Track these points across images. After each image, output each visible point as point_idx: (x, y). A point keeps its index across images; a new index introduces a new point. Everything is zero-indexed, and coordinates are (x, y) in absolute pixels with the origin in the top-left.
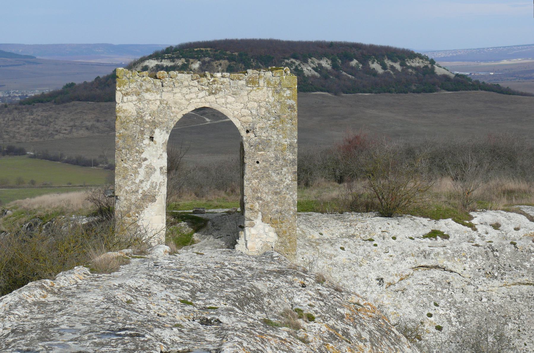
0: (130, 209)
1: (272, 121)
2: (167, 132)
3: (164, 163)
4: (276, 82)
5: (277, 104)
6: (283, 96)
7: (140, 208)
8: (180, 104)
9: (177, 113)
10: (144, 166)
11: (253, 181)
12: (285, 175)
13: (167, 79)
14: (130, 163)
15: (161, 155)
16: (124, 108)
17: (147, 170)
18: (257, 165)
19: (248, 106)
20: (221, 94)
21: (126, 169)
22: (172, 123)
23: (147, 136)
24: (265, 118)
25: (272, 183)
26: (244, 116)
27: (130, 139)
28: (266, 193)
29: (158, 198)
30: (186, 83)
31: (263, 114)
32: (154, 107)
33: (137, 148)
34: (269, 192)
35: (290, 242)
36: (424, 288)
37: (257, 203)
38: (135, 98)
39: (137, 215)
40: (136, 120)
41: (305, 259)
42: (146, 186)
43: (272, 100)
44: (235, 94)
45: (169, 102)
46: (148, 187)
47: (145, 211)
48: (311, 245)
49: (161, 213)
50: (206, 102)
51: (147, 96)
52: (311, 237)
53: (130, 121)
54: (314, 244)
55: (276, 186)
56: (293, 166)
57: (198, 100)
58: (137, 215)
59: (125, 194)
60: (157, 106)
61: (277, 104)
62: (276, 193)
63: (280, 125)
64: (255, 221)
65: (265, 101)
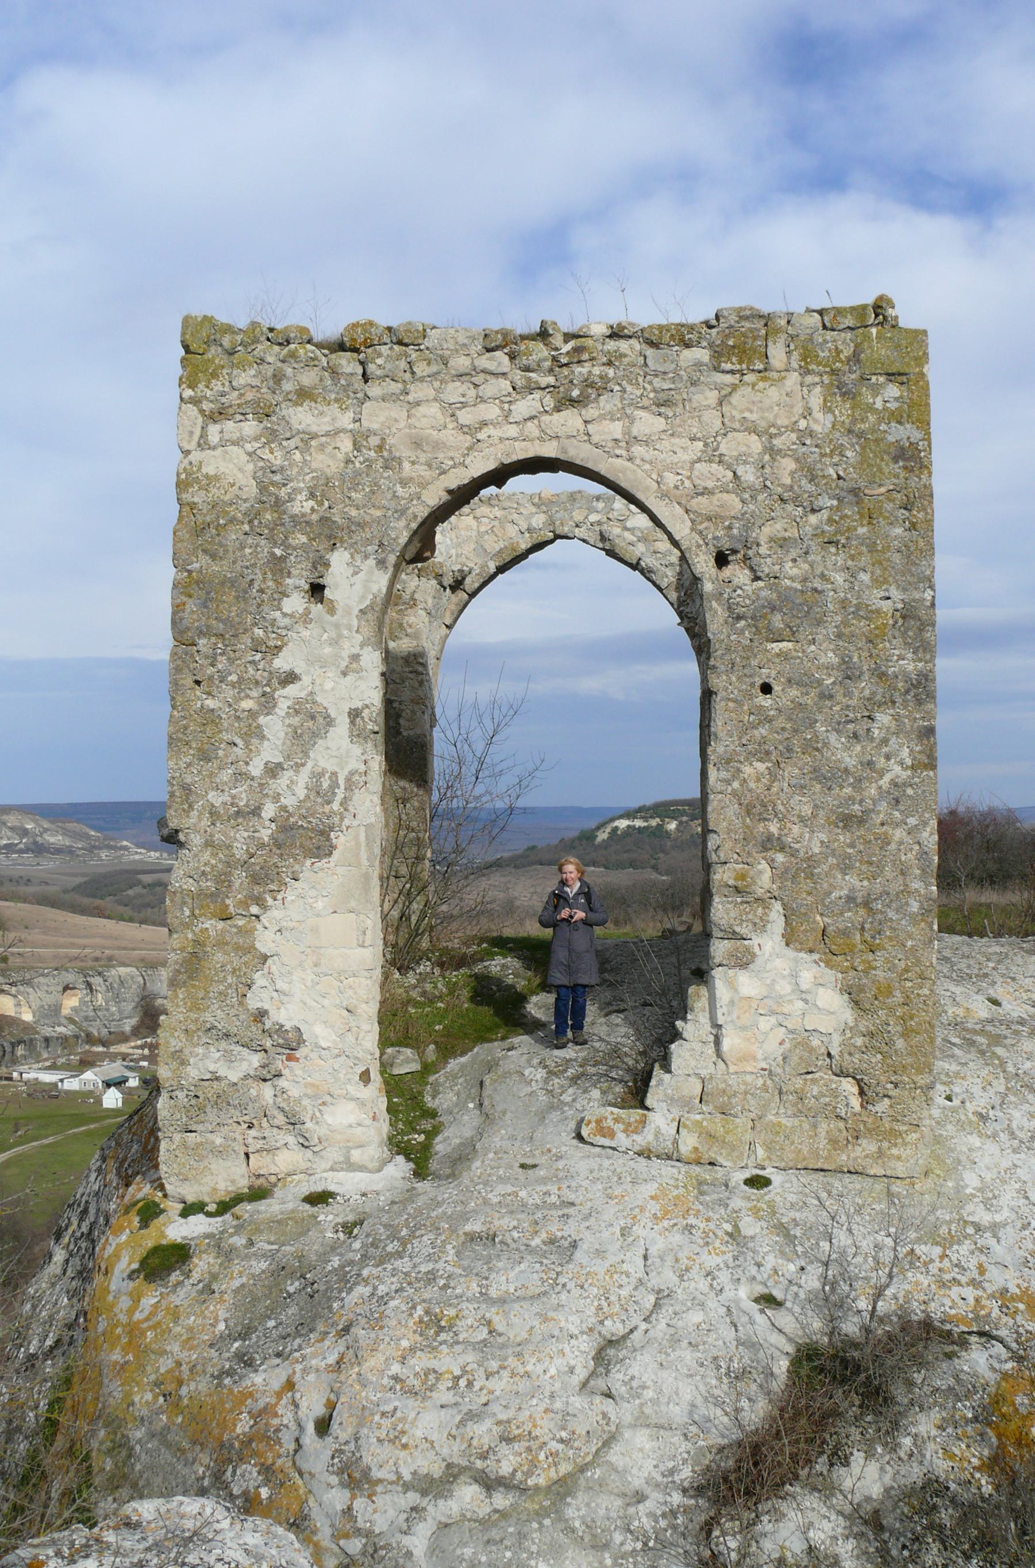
0: (223, 880)
1: (825, 515)
2: (381, 563)
3: (369, 691)
4: (838, 352)
5: (844, 441)
6: (871, 408)
7: (265, 880)
8: (437, 446)
9: (423, 485)
11: (747, 770)
12: (885, 741)
13: (384, 349)
14: (229, 693)
15: (355, 658)
16: (209, 469)
17: (296, 721)
18: (765, 701)
19: (723, 449)
20: (607, 403)
22: (402, 523)
23: (298, 580)
24: (797, 501)
25: (828, 777)
26: (706, 492)
27: (230, 596)
28: (802, 819)
29: (341, 840)
30: (461, 363)
31: (788, 481)
32: (326, 462)
33: (259, 632)
34: (814, 816)
35: (905, 1035)
37: (764, 865)
38: (250, 427)
39: (254, 910)
40: (252, 516)
41: (956, 1102)
42: (293, 790)
43: (821, 422)
44: (667, 403)
45: (390, 441)
46: (301, 793)
47: (290, 895)
48: (972, 1043)
49: (353, 904)
50: (546, 436)
51: (301, 417)
52: (961, 1012)
53: (232, 520)
54: (981, 1040)
55: (848, 791)
57: (512, 431)
58: (254, 910)
59: (205, 822)
60: (341, 456)
61: (844, 441)
62: (847, 821)
63: (862, 530)
64: (756, 941)
65: (793, 427)
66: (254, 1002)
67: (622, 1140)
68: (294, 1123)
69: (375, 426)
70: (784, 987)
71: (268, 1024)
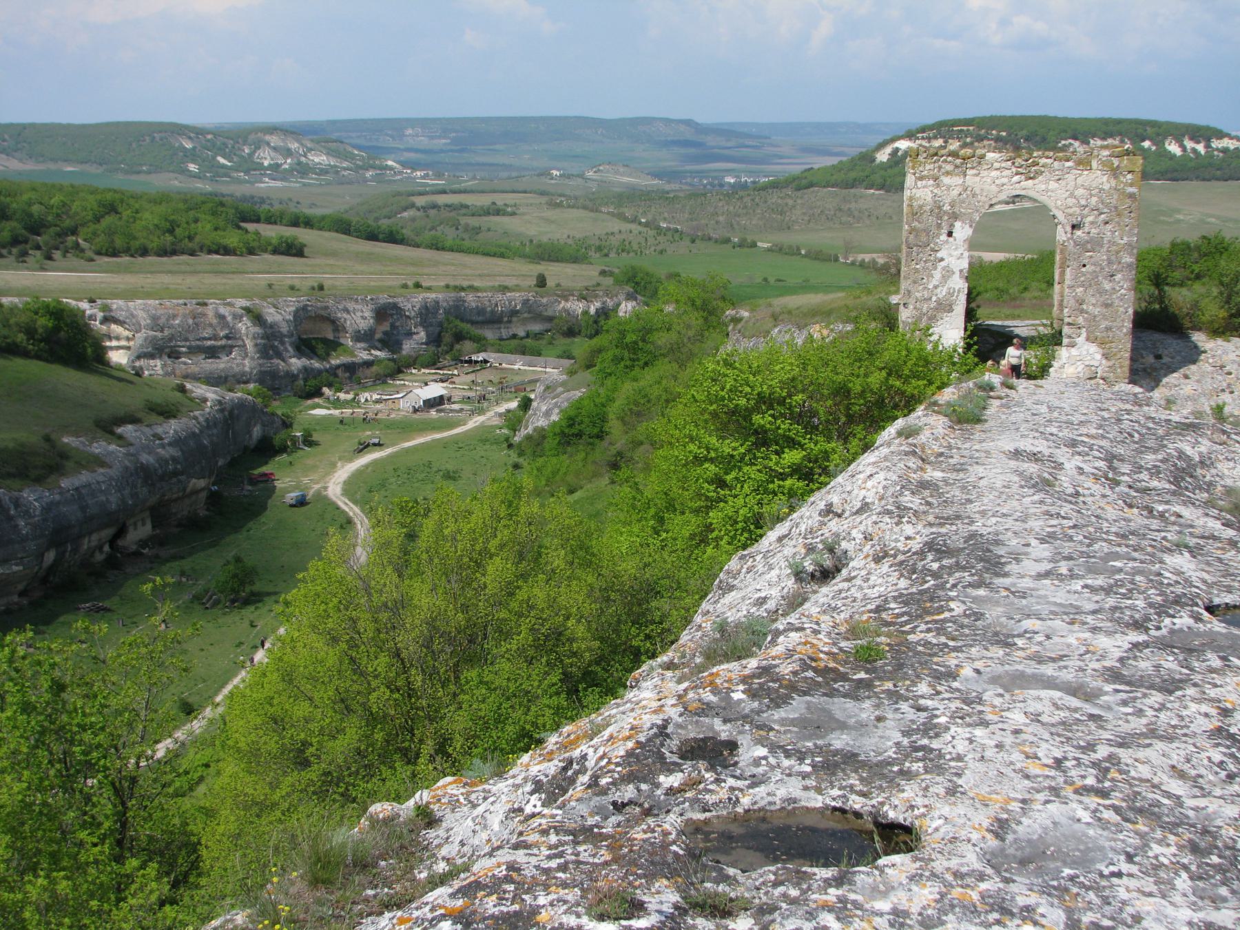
18: (1084, 269)
23: (945, 231)
25: (1102, 292)
30: (996, 165)
38: (931, 182)
42: (942, 292)
43: (1106, 187)
51: (946, 180)
62: (1107, 306)
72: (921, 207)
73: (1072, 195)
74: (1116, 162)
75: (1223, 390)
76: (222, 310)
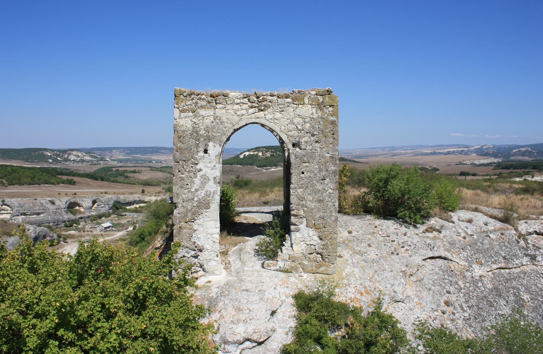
2: (220, 145)
3: (217, 173)
6: (326, 113)
10: (199, 176)
11: (299, 191)
12: (328, 184)
14: (187, 174)
15: (215, 166)
18: (302, 175)
21: (182, 179)
23: (202, 149)
26: (291, 131)
29: (211, 205)
30: (237, 101)
32: (208, 121)
36: (436, 277)
38: (191, 114)
42: (202, 194)
51: (202, 112)
56: (335, 176)
62: (320, 201)
66: (193, 240)
67: (272, 268)
68: (201, 266)
69: (218, 115)
70: (306, 235)
71: (196, 245)
72: (184, 131)
73: (292, 123)
74: (321, 99)
75: (392, 253)
76: (42, 201)
